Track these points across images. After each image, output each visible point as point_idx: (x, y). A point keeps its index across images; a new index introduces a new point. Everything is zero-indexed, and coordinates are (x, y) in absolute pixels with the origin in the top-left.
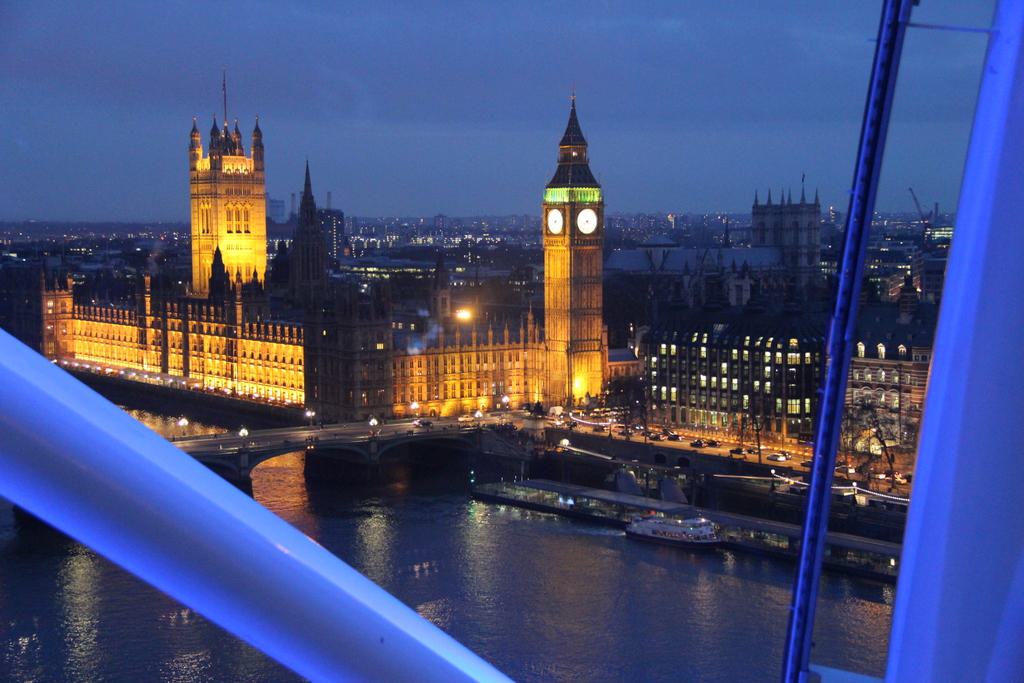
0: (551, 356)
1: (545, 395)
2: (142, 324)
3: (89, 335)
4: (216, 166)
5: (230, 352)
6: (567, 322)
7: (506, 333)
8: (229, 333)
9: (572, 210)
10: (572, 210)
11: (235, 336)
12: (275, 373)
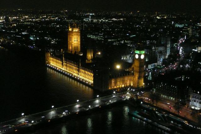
0: (134, 78)
1: (133, 84)
2: (62, 62)
3: (53, 61)
4: (72, 30)
5: (79, 71)
6: (138, 74)
7: (127, 74)
8: (79, 68)
9: (140, 55)
10: (140, 55)
11: (79, 68)
12: (87, 76)
